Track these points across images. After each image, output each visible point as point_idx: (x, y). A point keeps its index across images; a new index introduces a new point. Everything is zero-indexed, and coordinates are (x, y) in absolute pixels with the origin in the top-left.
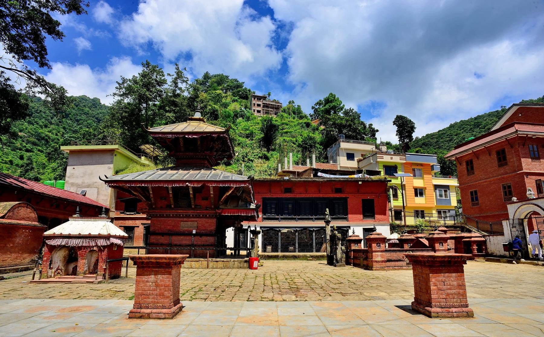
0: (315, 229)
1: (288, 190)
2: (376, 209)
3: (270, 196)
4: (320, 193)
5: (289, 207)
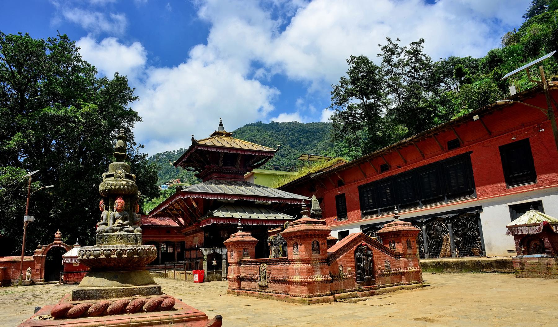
1: (385, 168)
2: (537, 160)
3: (365, 183)
5: (388, 191)
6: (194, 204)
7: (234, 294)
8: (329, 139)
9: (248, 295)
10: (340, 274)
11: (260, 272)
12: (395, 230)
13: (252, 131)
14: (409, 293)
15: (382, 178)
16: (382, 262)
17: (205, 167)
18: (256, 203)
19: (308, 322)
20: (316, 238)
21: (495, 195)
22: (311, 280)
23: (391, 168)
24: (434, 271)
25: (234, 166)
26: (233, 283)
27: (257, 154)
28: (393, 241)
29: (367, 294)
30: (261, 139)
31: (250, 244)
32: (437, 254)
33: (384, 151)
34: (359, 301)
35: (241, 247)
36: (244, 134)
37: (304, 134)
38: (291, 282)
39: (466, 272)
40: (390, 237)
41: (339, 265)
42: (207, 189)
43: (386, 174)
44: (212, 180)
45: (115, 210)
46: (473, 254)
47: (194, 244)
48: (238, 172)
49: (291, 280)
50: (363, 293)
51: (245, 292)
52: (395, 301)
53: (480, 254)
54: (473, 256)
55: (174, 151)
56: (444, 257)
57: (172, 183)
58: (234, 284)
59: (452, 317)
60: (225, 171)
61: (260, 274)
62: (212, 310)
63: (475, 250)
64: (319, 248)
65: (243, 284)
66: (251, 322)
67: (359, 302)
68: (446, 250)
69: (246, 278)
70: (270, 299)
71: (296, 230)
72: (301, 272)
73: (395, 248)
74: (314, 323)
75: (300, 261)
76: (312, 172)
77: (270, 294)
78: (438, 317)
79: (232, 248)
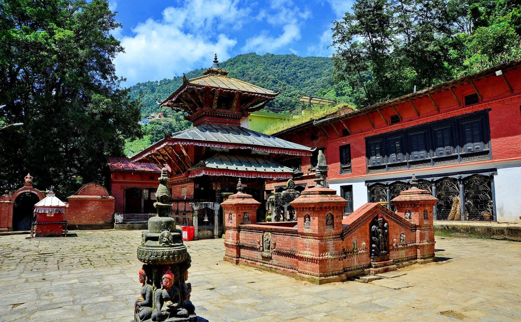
0: (436, 179)
3: (373, 134)
4: (439, 111)
5: (398, 145)
6: (184, 152)
7: (232, 263)
8: (328, 75)
9: (247, 265)
10: (353, 250)
11: (263, 241)
12: (413, 200)
13: (245, 63)
14: (424, 269)
15: (392, 130)
17: (197, 109)
18: (253, 153)
19: (326, 314)
20: (331, 210)
21: (512, 157)
22: (324, 257)
23: (402, 120)
24: (441, 235)
25: (229, 109)
26: (231, 249)
28: (409, 211)
29: (381, 271)
30: (254, 72)
31: (251, 207)
32: (445, 216)
33: (396, 101)
34: (374, 280)
35: (241, 211)
36: (235, 65)
37: (302, 69)
38: (300, 257)
39: (476, 238)
40: (407, 206)
42: (199, 136)
43: (397, 126)
44: (205, 124)
45: (162, 287)
46: (483, 218)
47: (182, 195)
49: (300, 255)
50: (377, 269)
51: (245, 261)
52: (413, 282)
53: (490, 218)
54: (483, 220)
55: (157, 82)
56: (453, 219)
57: (153, 117)
58: (232, 251)
59: (480, 311)
61: (263, 244)
62: (213, 289)
63: (485, 214)
64: (333, 222)
65: (242, 251)
66: (261, 310)
67: (373, 282)
68: (456, 212)
69: (246, 245)
70: (274, 272)
71: (310, 202)
72: (313, 248)
73: (411, 219)
74: (332, 315)
75: (311, 236)
76: (315, 118)
77: (274, 267)
78: (465, 309)
79: (231, 211)
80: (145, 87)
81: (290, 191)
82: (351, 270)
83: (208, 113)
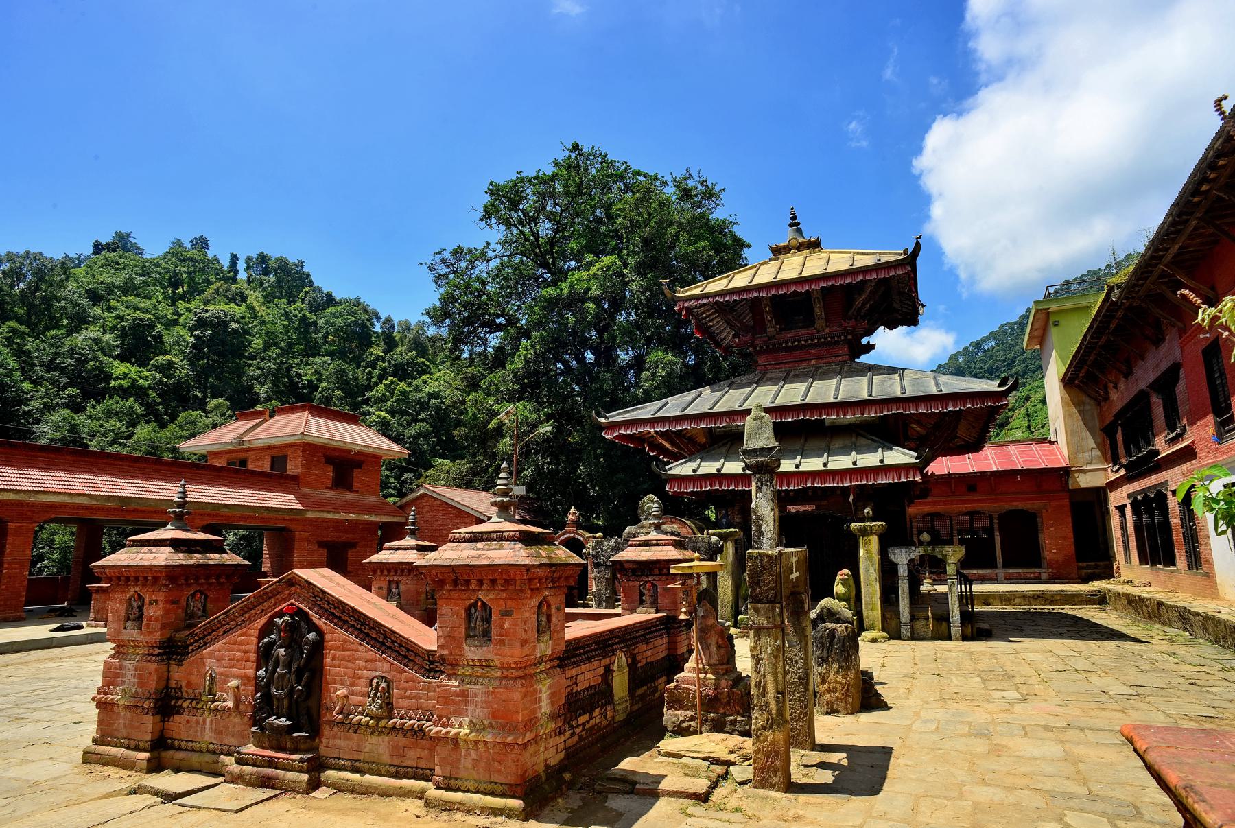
16: (360, 678)
18: (827, 423)
27: (849, 280)
31: (402, 571)
41: (207, 668)
48: (826, 338)
55: (1109, 266)
60: (787, 343)
64: (142, 614)
80: (1082, 286)
81: (643, 527)
82: (193, 750)
83: (761, 347)
